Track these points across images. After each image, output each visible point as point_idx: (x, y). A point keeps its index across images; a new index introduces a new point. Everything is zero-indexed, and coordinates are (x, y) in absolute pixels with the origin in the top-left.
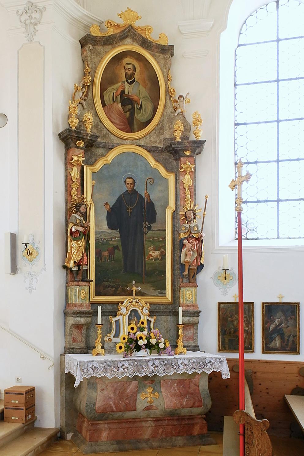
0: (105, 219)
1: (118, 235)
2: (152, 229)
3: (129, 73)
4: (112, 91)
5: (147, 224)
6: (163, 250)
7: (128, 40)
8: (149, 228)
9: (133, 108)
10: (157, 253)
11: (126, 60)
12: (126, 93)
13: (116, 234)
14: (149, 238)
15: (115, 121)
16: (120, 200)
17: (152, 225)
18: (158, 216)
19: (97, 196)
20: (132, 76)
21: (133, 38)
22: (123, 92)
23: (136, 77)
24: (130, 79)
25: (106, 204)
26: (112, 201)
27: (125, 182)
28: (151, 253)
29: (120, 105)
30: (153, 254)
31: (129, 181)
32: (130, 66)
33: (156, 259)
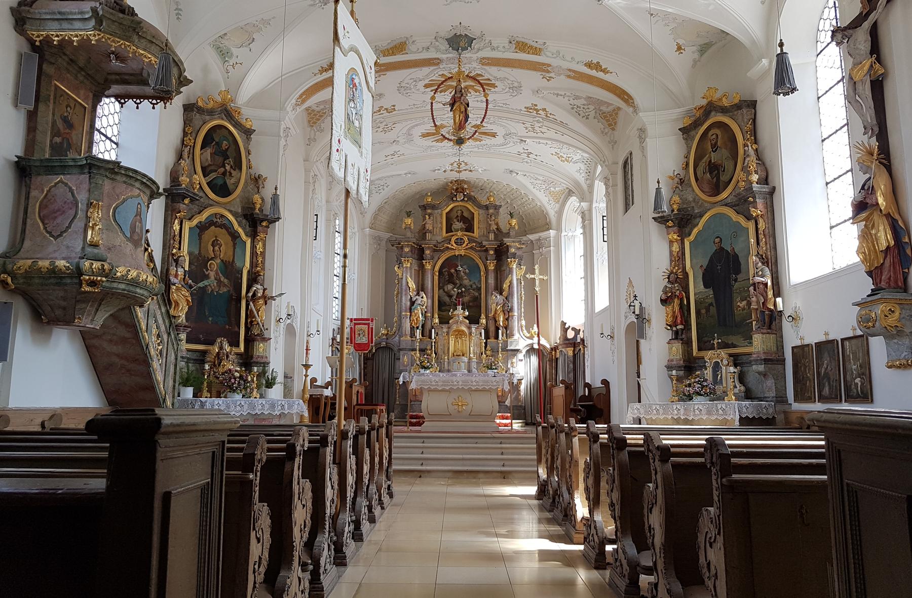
0: (701, 280)
1: (712, 292)
2: (738, 280)
3: (713, 142)
4: (703, 164)
5: (734, 276)
6: (749, 299)
7: (713, 113)
8: (736, 280)
9: (719, 173)
10: (744, 303)
11: (711, 133)
12: (713, 161)
13: (710, 292)
14: (736, 290)
15: (705, 190)
16: (711, 261)
17: (738, 276)
18: (743, 266)
19: (694, 261)
20: (716, 143)
21: (715, 110)
22: (711, 161)
23: (719, 143)
24: (715, 147)
25: (701, 266)
26: (705, 263)
27: (714, 242)
28: (739, 304)
29: (708, 174)
30: (741, 305)
31: (717, 240)
32: (714, 136)
33: (744, 309)
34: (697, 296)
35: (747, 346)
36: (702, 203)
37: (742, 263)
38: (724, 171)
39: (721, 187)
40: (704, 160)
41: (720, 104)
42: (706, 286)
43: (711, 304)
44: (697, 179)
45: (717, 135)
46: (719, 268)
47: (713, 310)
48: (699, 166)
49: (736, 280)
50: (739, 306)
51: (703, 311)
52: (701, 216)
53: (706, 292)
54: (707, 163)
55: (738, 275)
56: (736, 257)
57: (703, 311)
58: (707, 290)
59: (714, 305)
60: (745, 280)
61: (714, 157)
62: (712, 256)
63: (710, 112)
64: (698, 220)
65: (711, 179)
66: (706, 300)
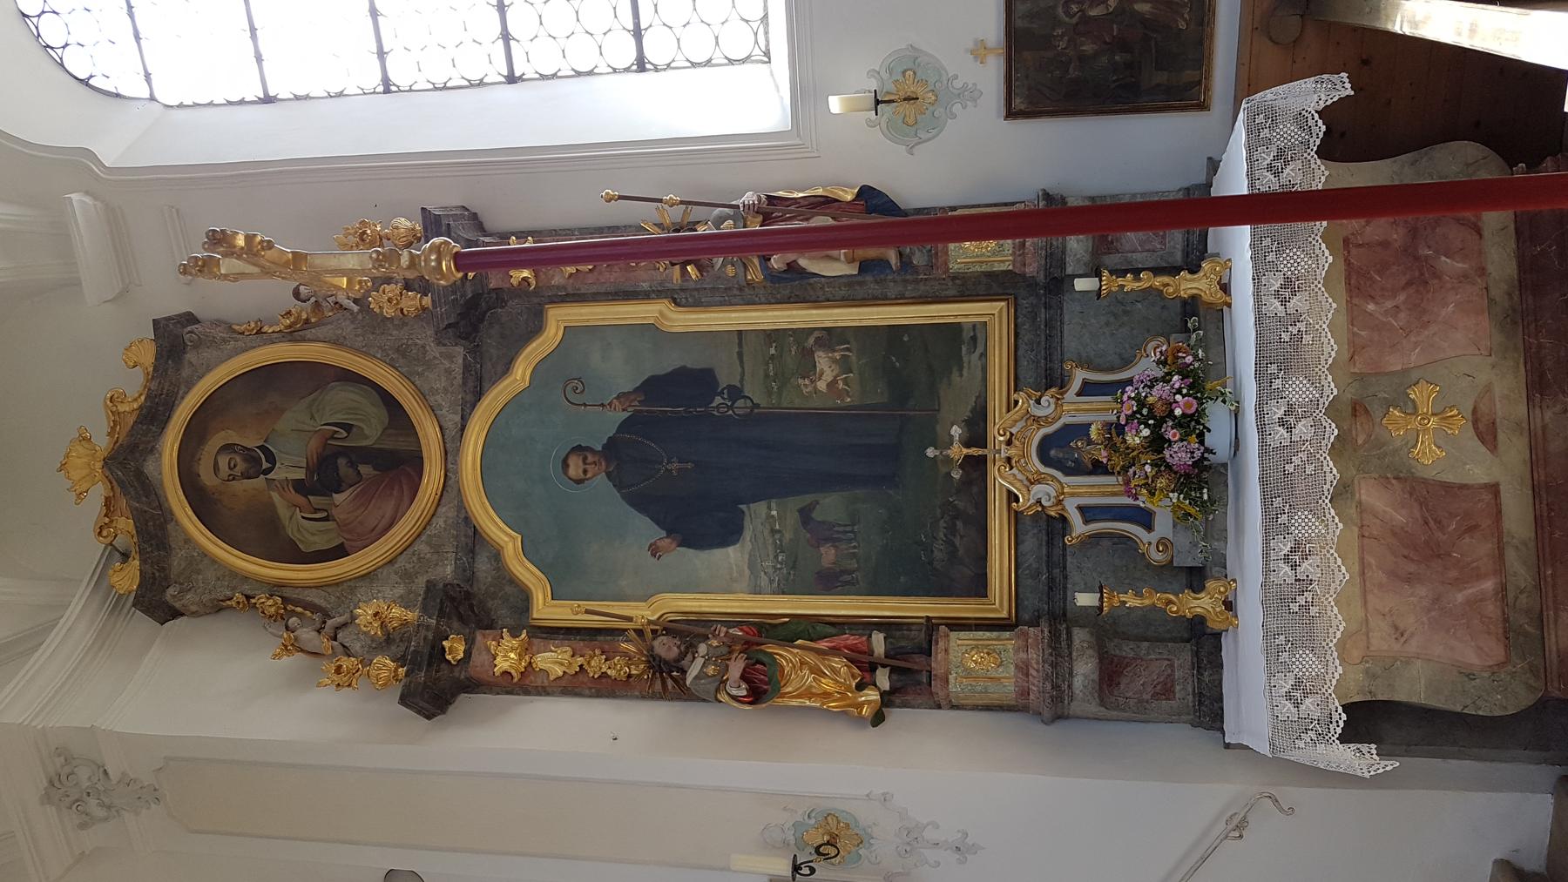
1: (760, 508)
3: (241, 466)
5: (718, 400)
6: (811, 340)
8: (735, 393)
9: (345, 451)
10: (823, 360)
11: (207, 477)
12: (300, 475)
13: (759, 516)
14: (769, 393)
15: (388, 515)
16: (640, 502)
20: (249, 456)
22: (299, 486)
23: (252, 442)
24: (258, 462)
25: (654, 551)
26: (645, 529)
27: (579, 482)
29: (339, 498)
30: (828, 376)
34: (764, 581)
35: (984, 355)
36: (428, 544)
37: (677, 364)
38: (348, 428)
39: (400, 444)
40: (283, 512)
41: (131, 420)
42: (728, 533)
43: (805, 515)
44: (339, 552)
45: (228, 448)
46: (675, 466)
47: (831, 506)
48: (295, 536)
49: (735, 393)
50: (832, 385)
51: (828, 555)
52: (473, 539)
53: (755, 538)
54: (300, 499)
55: (716, 383)
56: (654, 388)
57: (828, 555)
58: (748, 534)
59: (808, 499)
60: (740, 355)
61: (289, 469)
62: (624, 497)
63: (140, 475)
64: (483, 566)
65: (358, 488)
66: (788, 536)
